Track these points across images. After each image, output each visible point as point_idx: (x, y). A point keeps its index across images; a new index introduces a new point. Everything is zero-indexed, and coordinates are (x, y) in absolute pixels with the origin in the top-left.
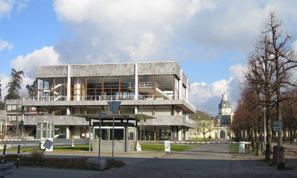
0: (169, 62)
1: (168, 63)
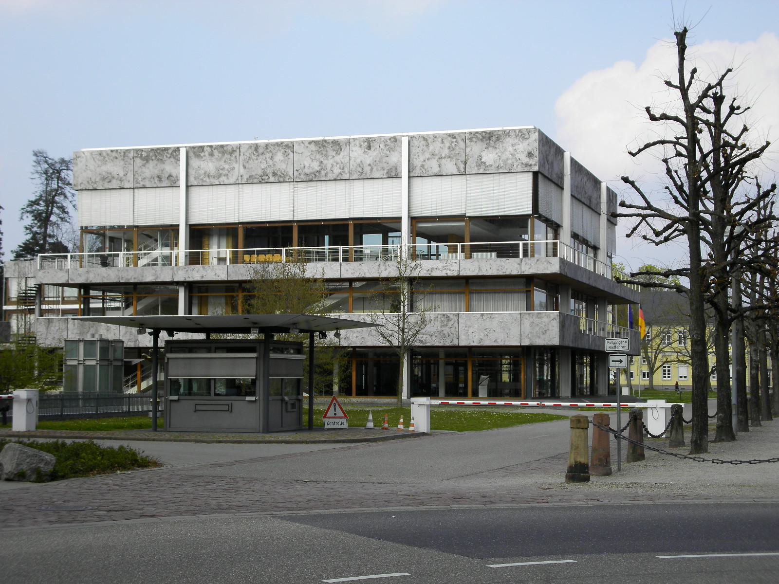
0: (515, 130)
1: (512, 134)
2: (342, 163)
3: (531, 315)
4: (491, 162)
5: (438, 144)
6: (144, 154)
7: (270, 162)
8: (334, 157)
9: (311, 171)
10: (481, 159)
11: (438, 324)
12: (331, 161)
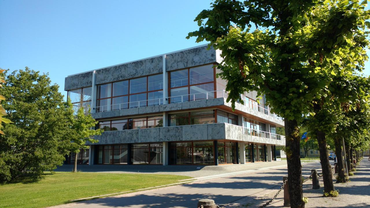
2: (143, 69)
3: (212, 125)
4: (197, 61)
5: (177, 56)
6: (84, 75)
7: (120, 72)
8: (140, 67)
9: (133, 74)
10: (193, 60)
11: (174, 131)
12: (139, 69)
